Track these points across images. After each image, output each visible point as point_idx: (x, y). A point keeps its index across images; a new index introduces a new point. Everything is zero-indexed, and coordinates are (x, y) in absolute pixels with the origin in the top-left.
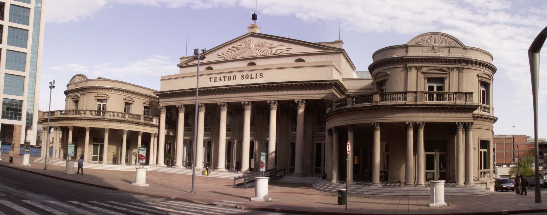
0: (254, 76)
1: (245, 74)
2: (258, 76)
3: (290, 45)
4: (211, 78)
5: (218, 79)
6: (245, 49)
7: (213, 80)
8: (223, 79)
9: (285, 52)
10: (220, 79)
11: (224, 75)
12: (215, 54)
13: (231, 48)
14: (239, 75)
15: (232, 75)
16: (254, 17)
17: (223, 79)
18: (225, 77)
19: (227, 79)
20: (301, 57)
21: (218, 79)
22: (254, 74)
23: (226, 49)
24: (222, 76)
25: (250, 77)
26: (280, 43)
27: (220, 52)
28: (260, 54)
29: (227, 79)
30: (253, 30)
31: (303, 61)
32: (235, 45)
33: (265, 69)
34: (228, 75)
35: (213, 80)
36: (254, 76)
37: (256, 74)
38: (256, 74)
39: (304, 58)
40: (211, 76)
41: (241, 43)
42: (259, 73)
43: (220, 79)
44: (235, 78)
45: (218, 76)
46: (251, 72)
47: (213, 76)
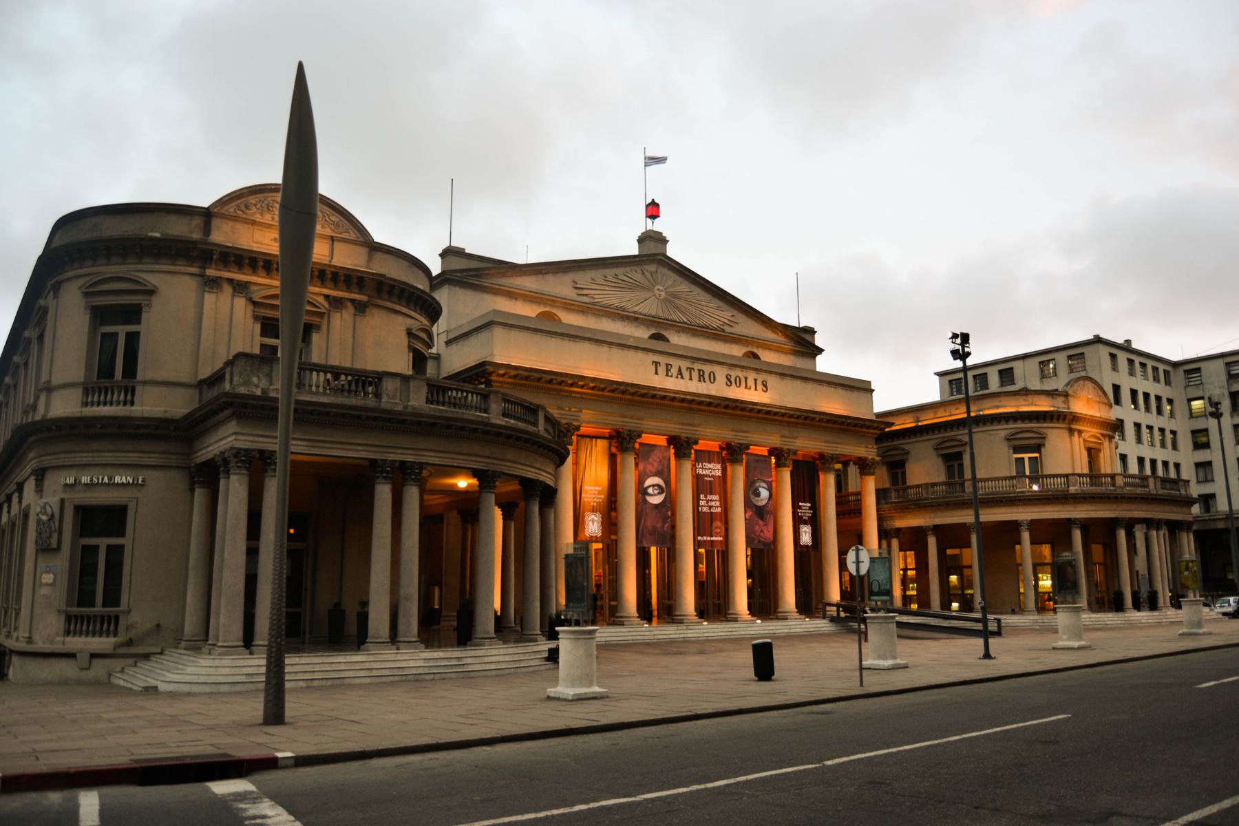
0: (751, 383)
1: (734, 373)
2: (760, 386)
3: (735, 312)
4: (656, 364)
5: (674, 371)
7: (662, 370)
8: (686, 374)
9: (727, 329)
12: (569, 278)
13: (610, 278)
14: (721, 373)
15: (707, 368)
16: (653, 210)
17: (686, 374)
18: (690, 370)
19: (695, 375)
20: (755, 350)
21: (674, 371)
22: (751, 376)
23: (598, 274)
24: (684, 364)
26: (716, 303)
27: (584, 278)
28: (676, 316)
30: (652, 248)
31: (756, 356)
33: (771, 372)
34: (697, 366)
36: (751, 383)
39: (760, 352)
40: (657, 358)
41: (635, 274)
45: (676, 363)
47: (663, 360)
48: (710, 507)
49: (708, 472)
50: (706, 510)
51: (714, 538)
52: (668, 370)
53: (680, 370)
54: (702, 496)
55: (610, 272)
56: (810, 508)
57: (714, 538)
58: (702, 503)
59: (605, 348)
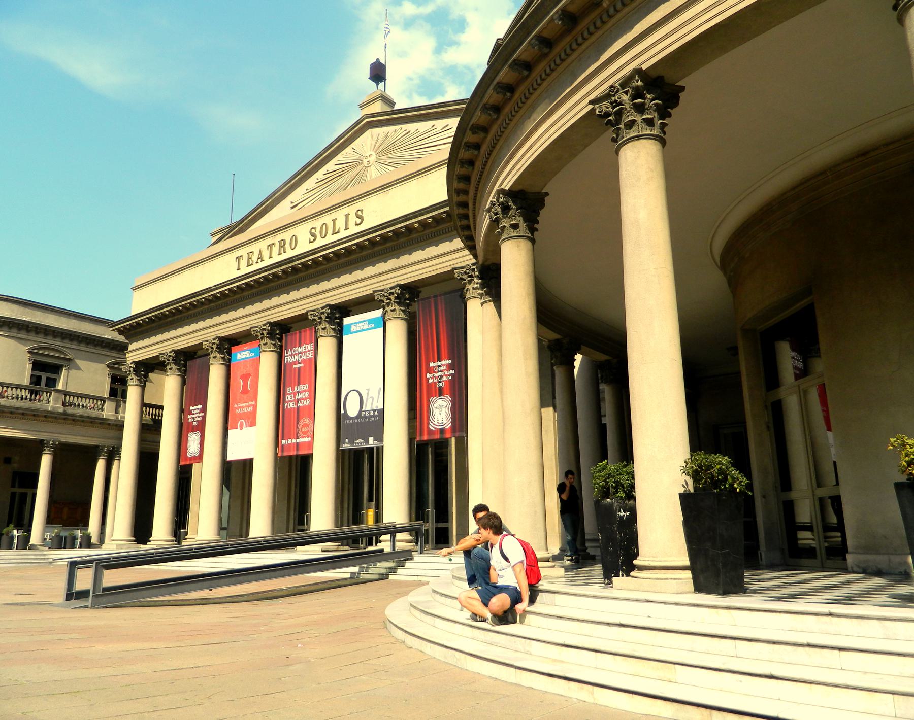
0: (341, 224)
1: (317, 223)
2: (353, 219)
5: (255, 258)
6: (354, 172)
8: (266, 254)
10: (260, 258)
11: (269, 241)
12: (286, 204)
14: (302, 232)
15: (286, 235)
19: (275, 250)
21: (255, 258)
25: (330, 231)
27: (297, 195)
29: (275, 250)
32: (330, 166)
35: (244, 262)
36: (341, 224)
37: (347, 216)
38: (347, 216)
40: (237, 253)
42: (351, 210)
43: (260, 258)
44: (295, 241)
45: (255, 248)
46: (334, 215)
48: (298, 400)
49: (297, 358)
50: (292, 405)
51: (298, 441)
52: (249, 258)
53: (260, 253)
54: (289, 390)
55: (320, 174)
56: (450, 367)
57: (300, 440)
58: (289, 398)
59: (200, 268)
